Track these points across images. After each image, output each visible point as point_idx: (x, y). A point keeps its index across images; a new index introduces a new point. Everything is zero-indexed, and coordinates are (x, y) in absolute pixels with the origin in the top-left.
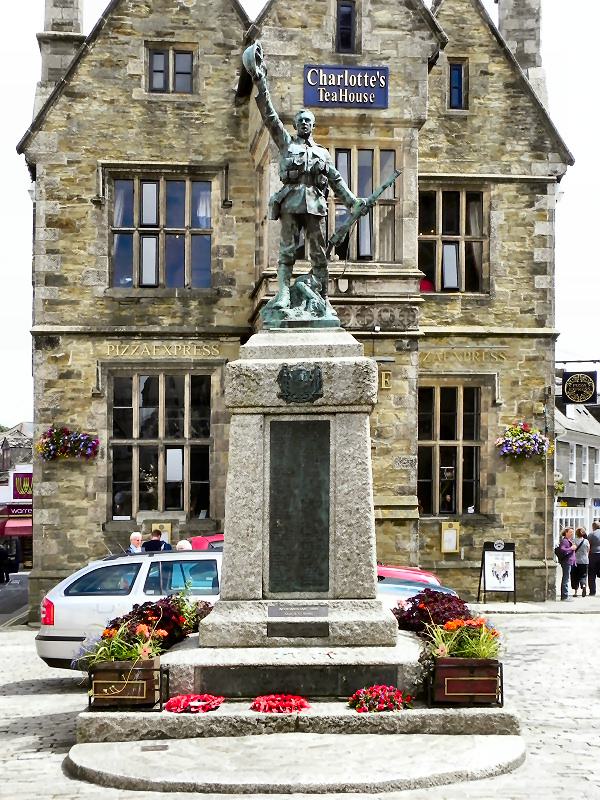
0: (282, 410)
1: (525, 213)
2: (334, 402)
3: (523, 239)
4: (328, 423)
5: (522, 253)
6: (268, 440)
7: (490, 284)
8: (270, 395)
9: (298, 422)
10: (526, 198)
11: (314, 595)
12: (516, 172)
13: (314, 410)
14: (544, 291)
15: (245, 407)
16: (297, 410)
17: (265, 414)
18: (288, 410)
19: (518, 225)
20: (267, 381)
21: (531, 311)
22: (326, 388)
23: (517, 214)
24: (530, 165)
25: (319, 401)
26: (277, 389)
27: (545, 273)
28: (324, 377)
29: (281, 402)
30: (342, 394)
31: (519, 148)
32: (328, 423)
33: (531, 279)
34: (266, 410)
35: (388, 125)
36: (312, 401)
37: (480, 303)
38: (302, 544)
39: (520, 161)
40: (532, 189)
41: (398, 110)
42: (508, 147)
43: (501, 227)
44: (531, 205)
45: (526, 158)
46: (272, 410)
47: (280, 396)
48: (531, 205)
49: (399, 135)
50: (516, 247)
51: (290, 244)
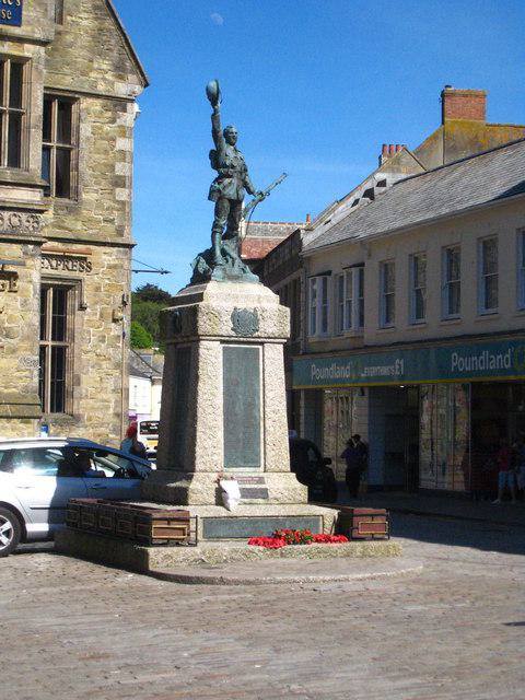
1: (107, 128)
3: (106, 152)
5: (106, 165)
7: (77, 193)
8: (226, 328)
10: (109, 114)
11: (252, 469)
12: (101, 88)
14: (123, 203)
19: (102, 139)
21: (112, 221)
22: (261, 324)
23: (101, 128)
24: (113, 84)
27: (124, 186)
29: (233, 333)
31: (104, 67)
33: (112, 193)
35: (20, 40)
37: (73, 211)
38: (244, 433)
39: (104, 79)
40: (115, 106)
41: (29, 28)
42: (96, 66)
43: (88, 138)
44: (113, 121)
45: (109, 76)
48: (113, 121)
49: (28, 51)
50: (100, 158)
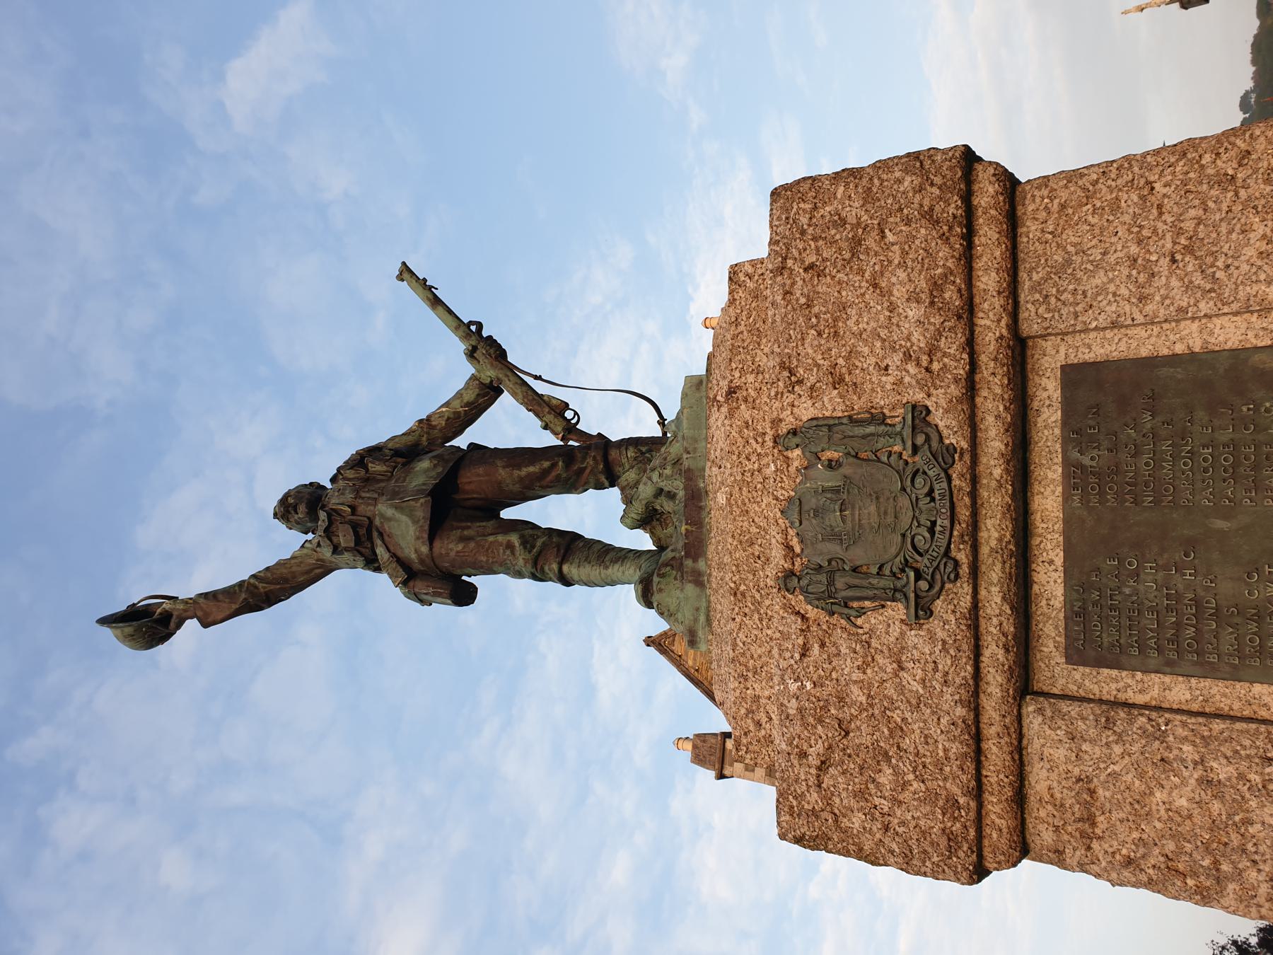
0: (994, 601)
2: (952, 345)
4: (1073, 375)
6: (1180, 691)
9: (1070, 522)
13: (995, 442)
15: (978, 792)
16: (994, 530)
17: (1024, 684)
18: (995, 573)
20: (848, 667)
25: (947, 423)
26: (887, 620)
28: (832, 404)
30: (914, 312)
32: (1073, 375)
34: (995, 684)
36: (945, 456)
46: (994, 652)
47: (922, 610)
51: (510, 546)
